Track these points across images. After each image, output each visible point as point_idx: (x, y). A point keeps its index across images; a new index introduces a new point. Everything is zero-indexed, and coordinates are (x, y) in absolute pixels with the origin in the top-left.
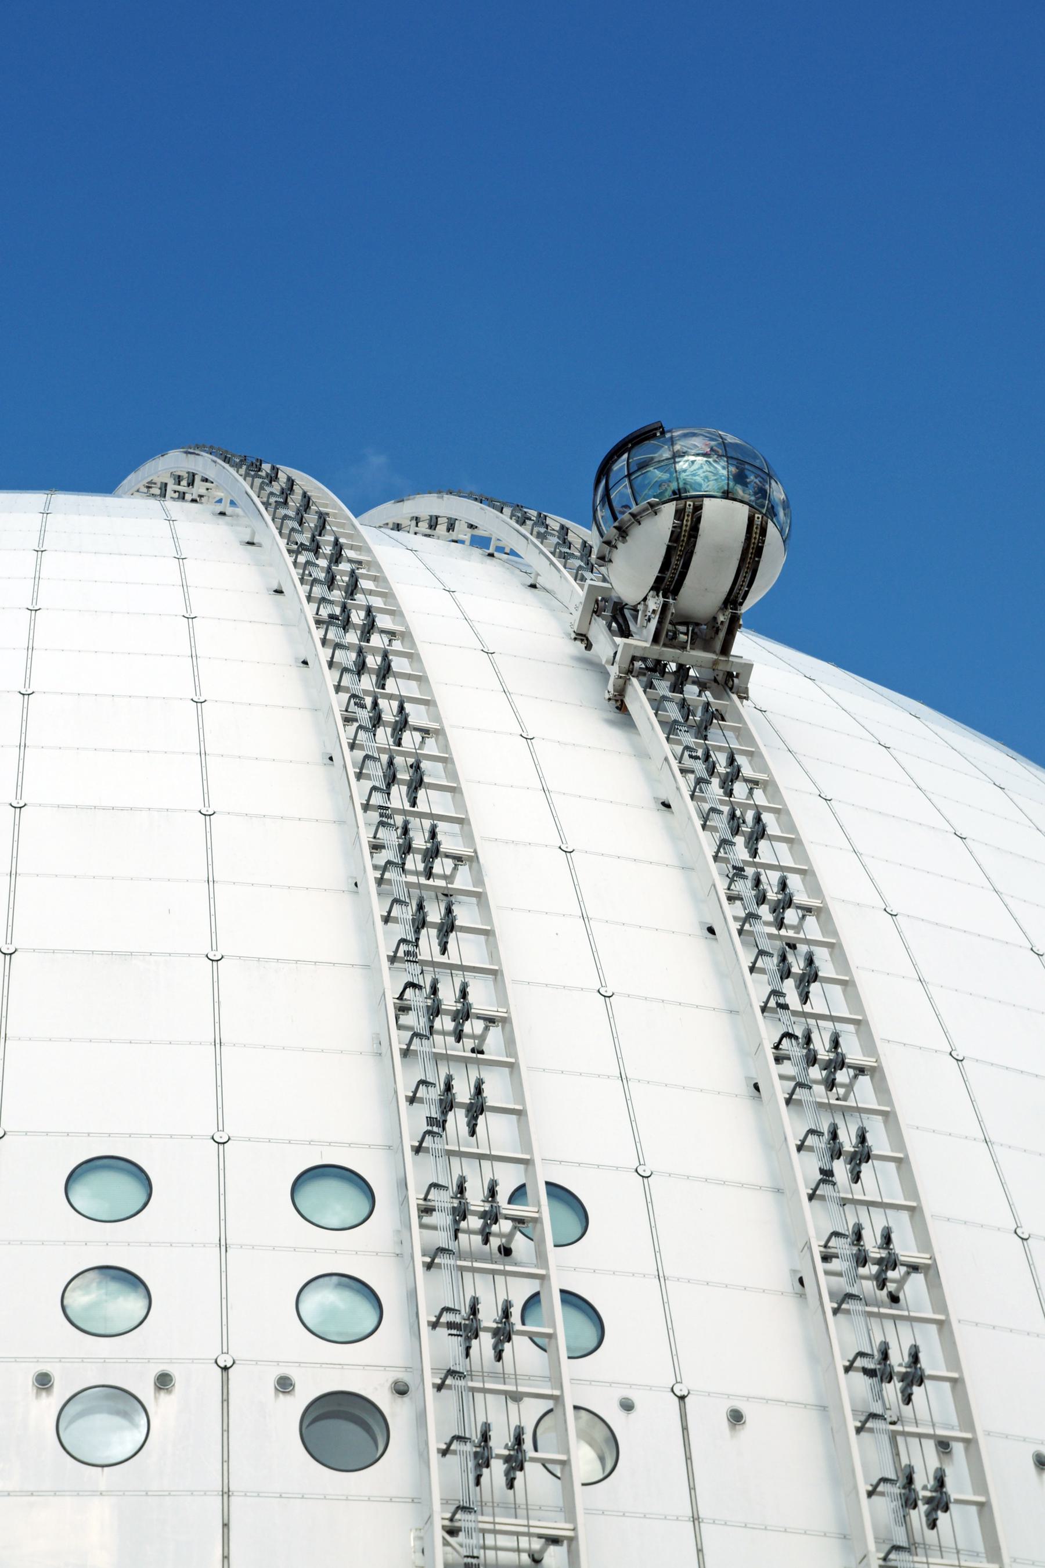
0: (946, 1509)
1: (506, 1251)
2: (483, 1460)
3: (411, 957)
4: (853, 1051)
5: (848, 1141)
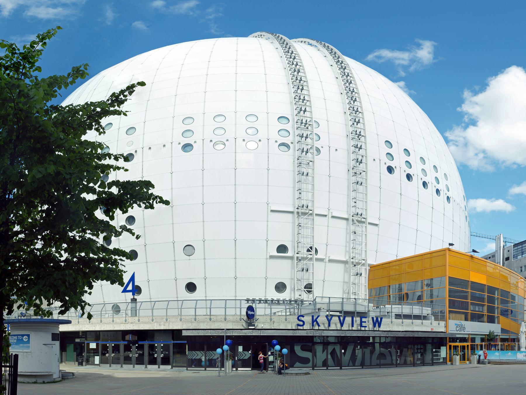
0: (362, 163)
1: (307, 128)
2: (303, 152)
3: (297, 92)
4: (360, 110)
5: (357, 120)
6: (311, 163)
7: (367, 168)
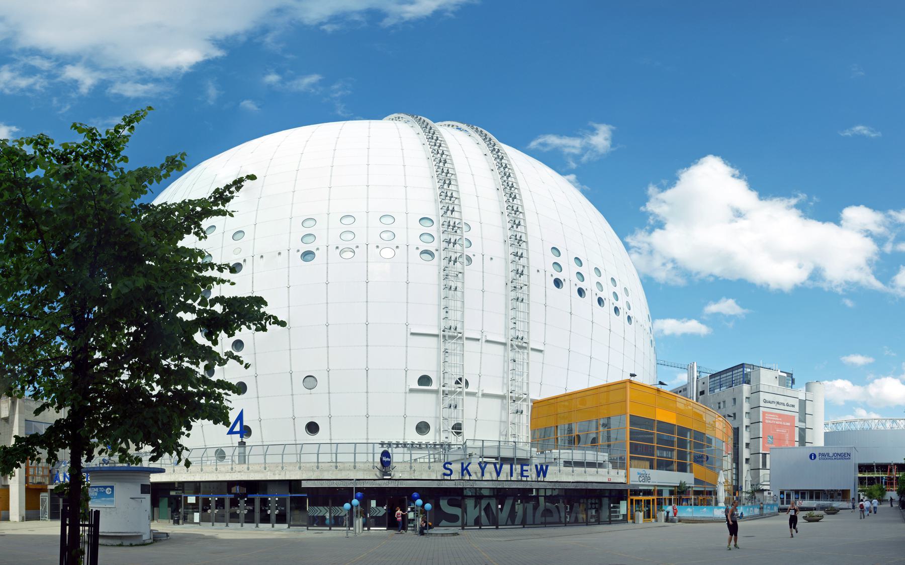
1: (456, 232)
2: (450, 261)
3: (443, 188)
5: (517, 222)
6: (460, 275)
7: (529, 281)
